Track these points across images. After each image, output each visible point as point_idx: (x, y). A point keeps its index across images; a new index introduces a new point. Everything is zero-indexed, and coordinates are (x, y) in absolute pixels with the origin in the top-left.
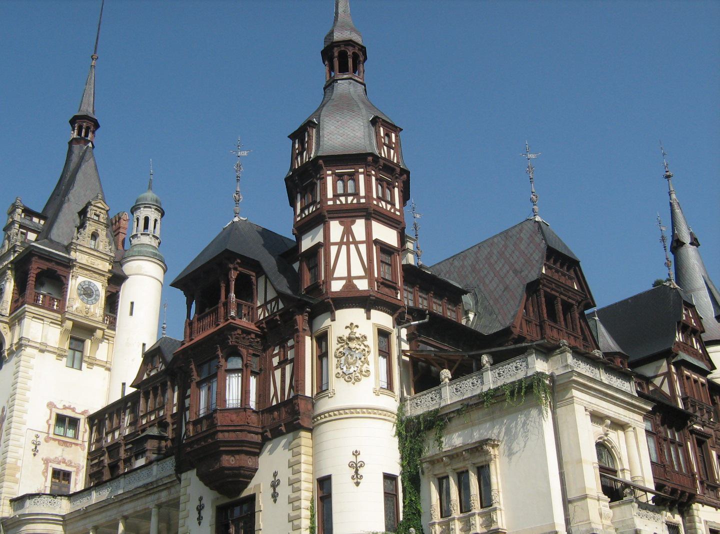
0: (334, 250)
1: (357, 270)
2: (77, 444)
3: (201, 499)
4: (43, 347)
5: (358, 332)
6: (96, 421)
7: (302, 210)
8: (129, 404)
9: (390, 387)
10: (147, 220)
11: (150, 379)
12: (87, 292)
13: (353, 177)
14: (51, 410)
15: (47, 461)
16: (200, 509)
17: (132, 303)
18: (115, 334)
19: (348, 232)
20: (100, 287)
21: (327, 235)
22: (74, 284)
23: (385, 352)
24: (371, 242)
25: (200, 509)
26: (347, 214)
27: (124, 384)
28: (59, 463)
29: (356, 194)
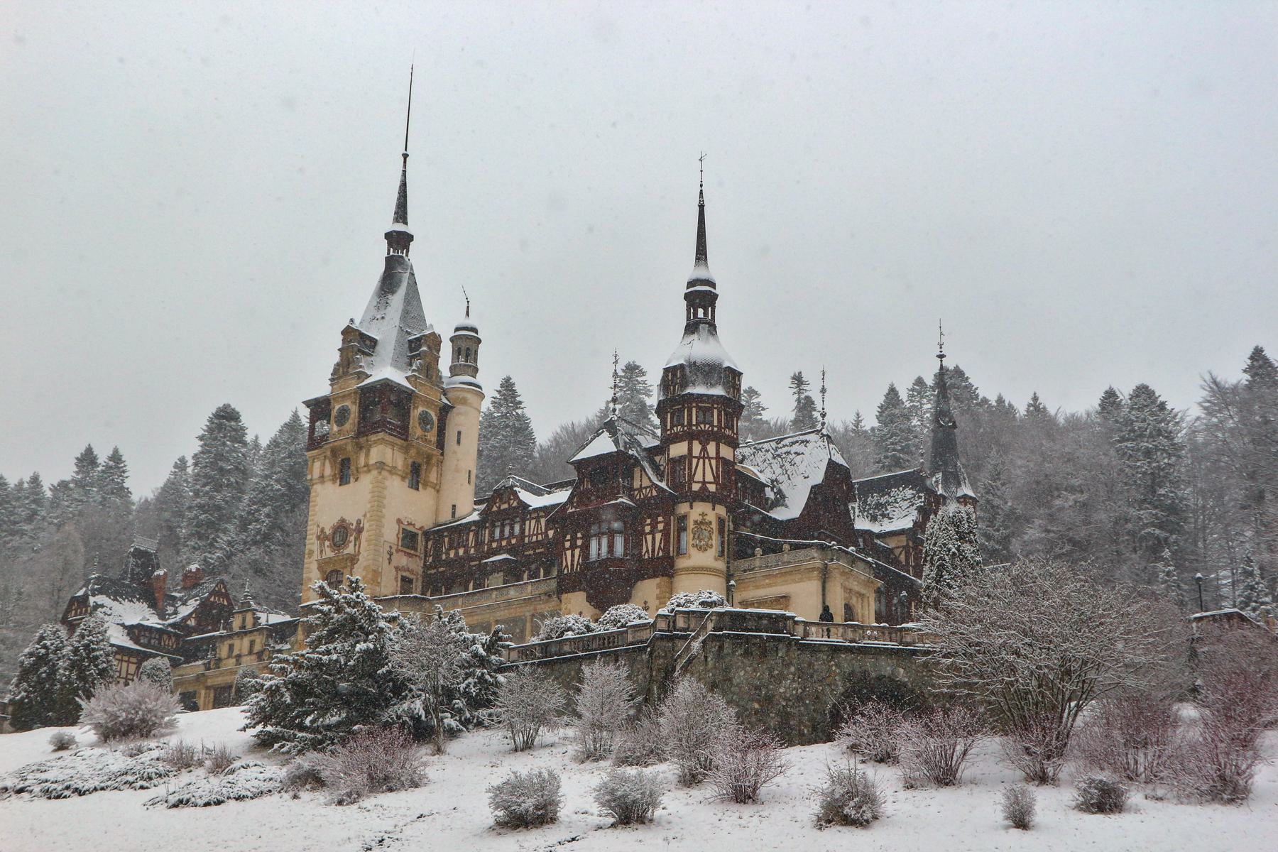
0: (695, 461)
1: (709, 478)
5: (708, 518)
9: (722, 553)
11: (500, 511)
12: (424, 419)
13: (711, 410)
15: (397, 568)
17: (459, 433)
19: (704, 449)
20: (434, 416)
21: (690, 450)
22: (416, 413)
23: (721, 532)
24: (718, 457)
26: (704, 438)
29: (711, 424)
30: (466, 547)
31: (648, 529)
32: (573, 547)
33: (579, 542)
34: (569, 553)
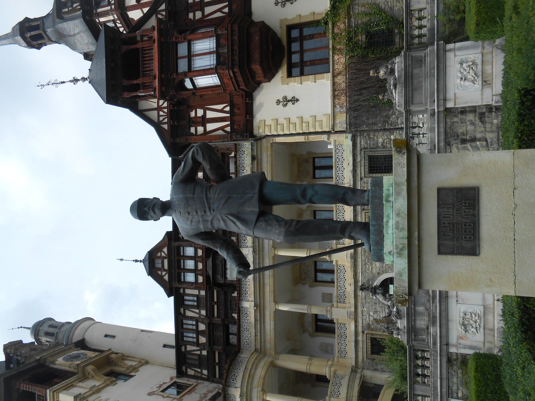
2: (196, 386)
3: (278, 102)
4: (94, 389)
6: (184, 368)
7: (109, 4)
8: (182, 310)
10: (50, 326)
11: (169, 271)
14: (155, 394)
16: (286, 101)
17: (106, 336)
18: (122, 354)
25: (286, 101)
27: (165, 346)
28: (206, 397)
30: (197, 321)
31: (199, 15)
32: (204, 121)
33: (200, 113)
34: (210, 127)
